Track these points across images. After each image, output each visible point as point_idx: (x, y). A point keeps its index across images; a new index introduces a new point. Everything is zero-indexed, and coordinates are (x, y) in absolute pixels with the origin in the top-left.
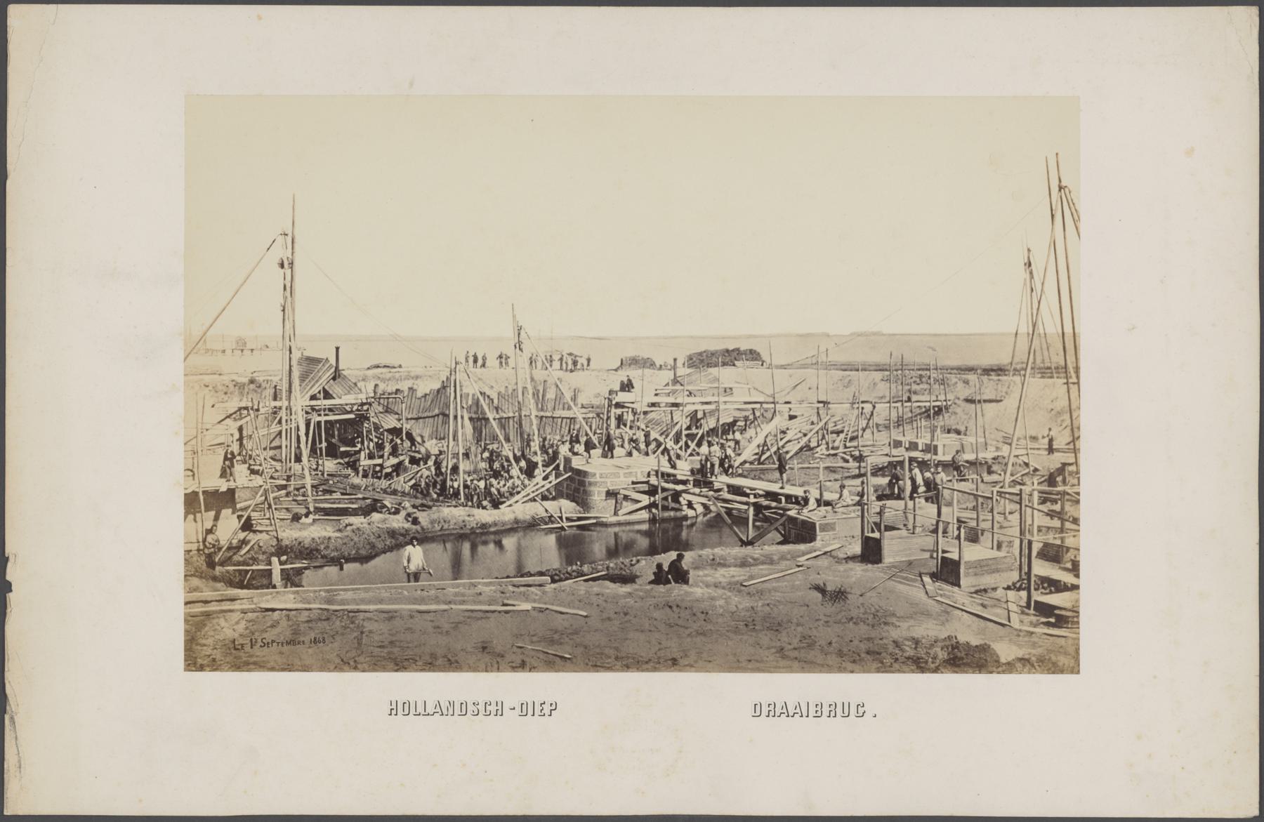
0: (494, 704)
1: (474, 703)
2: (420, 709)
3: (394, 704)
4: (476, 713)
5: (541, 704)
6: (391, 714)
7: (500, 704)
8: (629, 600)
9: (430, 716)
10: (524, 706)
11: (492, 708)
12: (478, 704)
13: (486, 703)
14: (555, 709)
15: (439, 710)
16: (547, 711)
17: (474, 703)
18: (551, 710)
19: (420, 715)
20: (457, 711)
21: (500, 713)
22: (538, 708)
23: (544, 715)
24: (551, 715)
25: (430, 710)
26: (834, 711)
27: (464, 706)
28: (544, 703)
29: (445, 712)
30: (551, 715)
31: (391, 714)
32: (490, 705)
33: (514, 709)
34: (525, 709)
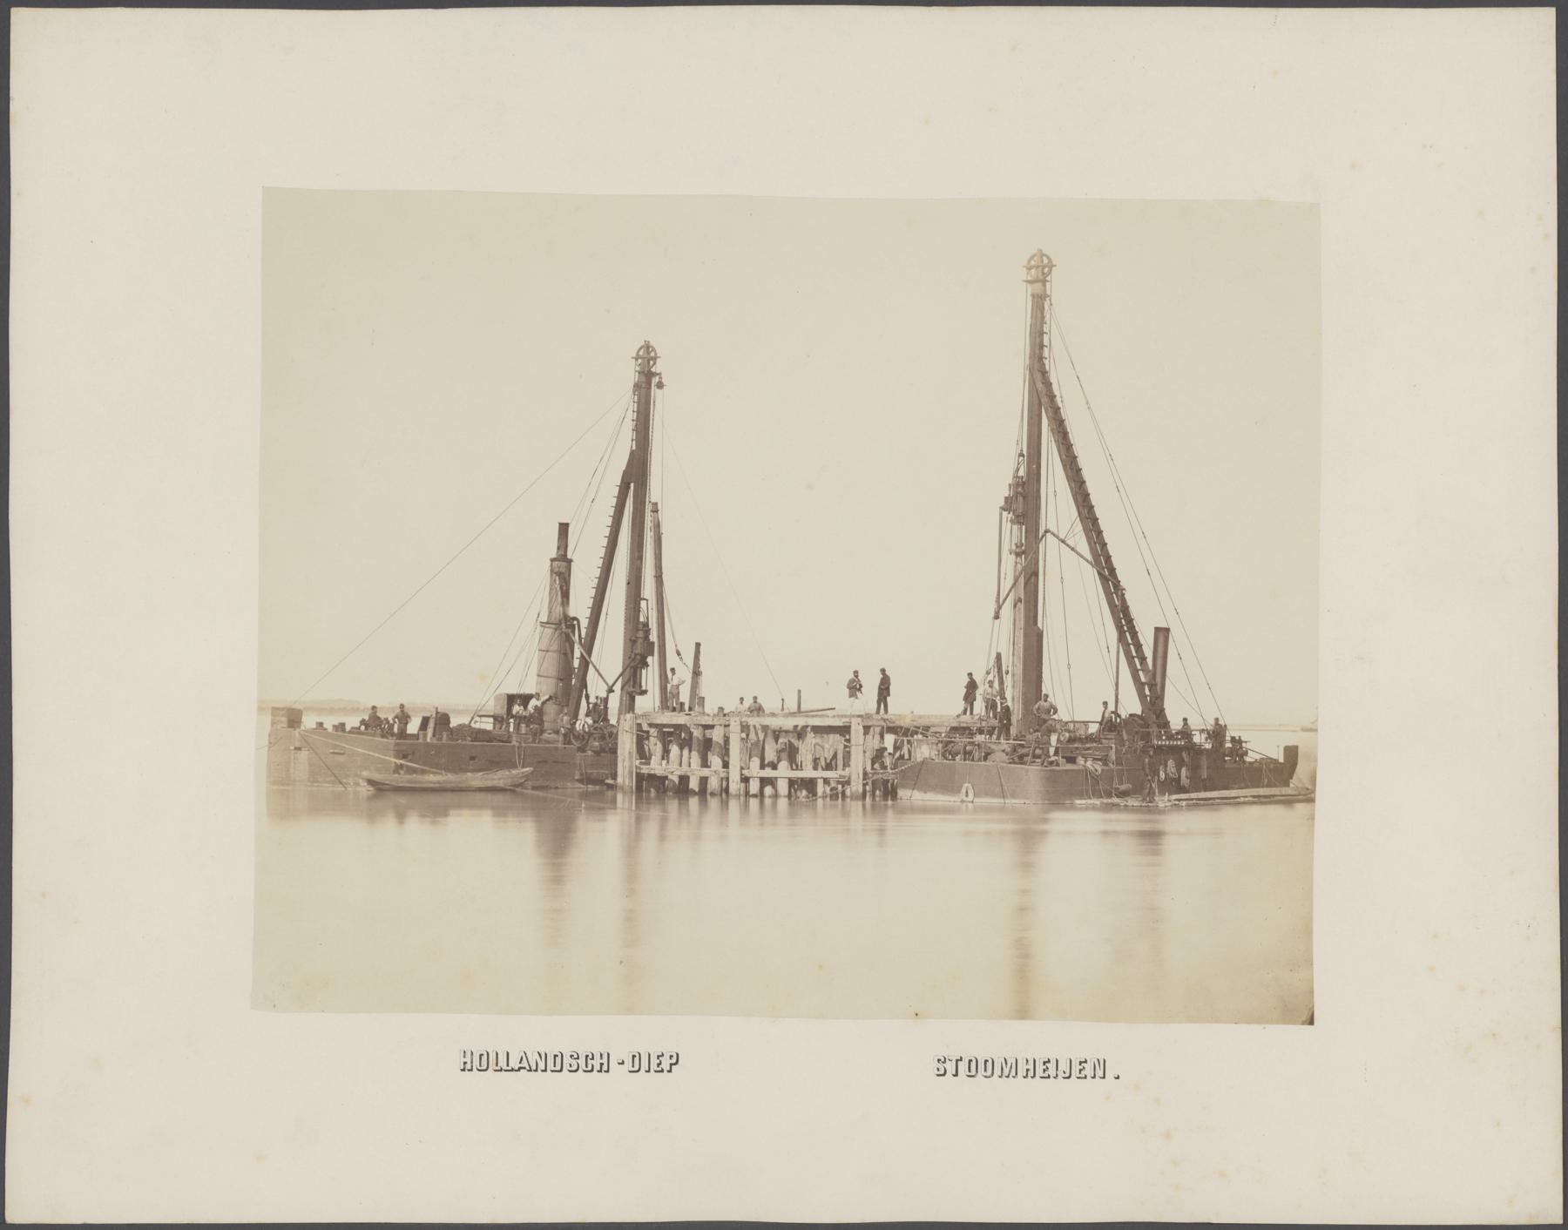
0: (597, 1056)
2: (502, 1063)
9: (514, 1073)
13: (587, 1056)
14: (677, 1063)
16: (665, 1065)
18: (671, 1065)
19: (501, 1070)
22: (654, 1061)
24: (670, 1071)
25: (514, 1063)
30: (670, 1071)
34: (637, 1063)
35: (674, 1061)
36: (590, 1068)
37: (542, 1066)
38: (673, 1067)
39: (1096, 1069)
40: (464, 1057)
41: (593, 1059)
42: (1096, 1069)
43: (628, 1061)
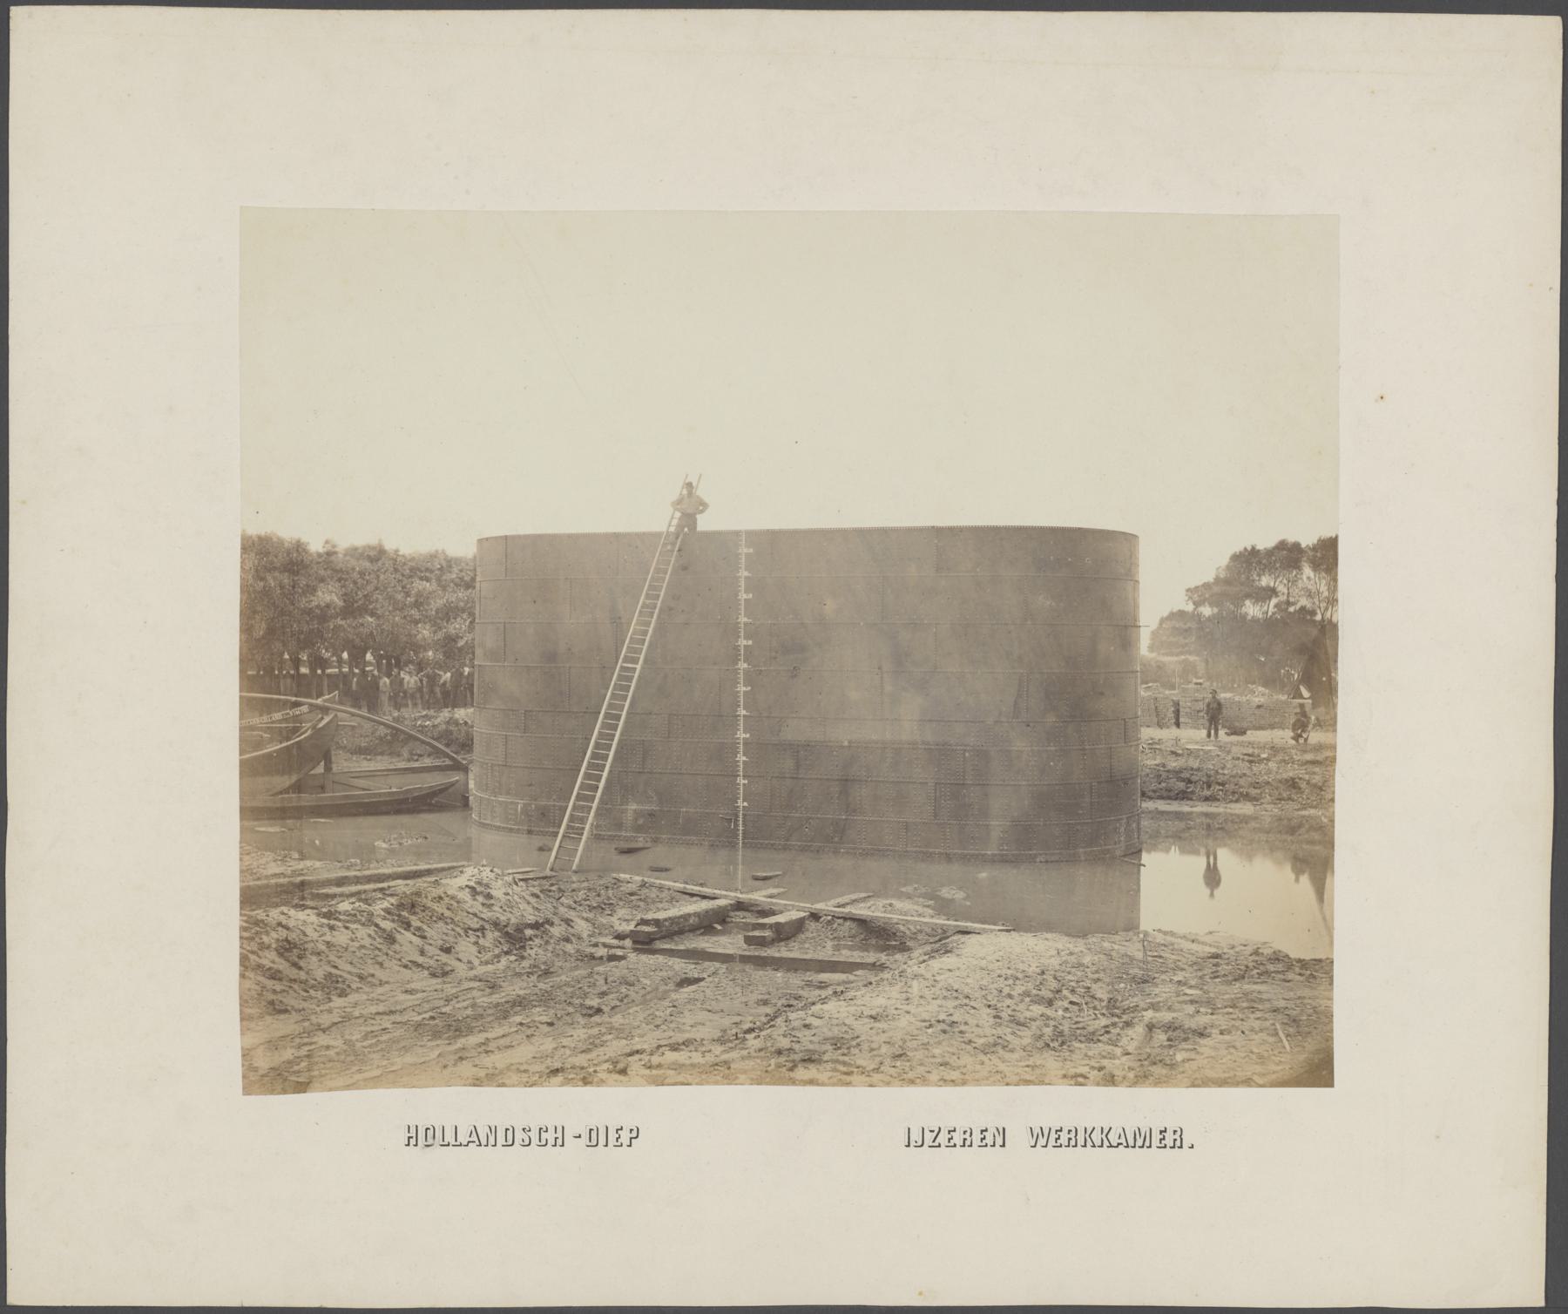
0: (552, 1130)
1: (524, 1129)
2: (449, 1138)
3: (413, 1130)
4: (527, 1143)
5: (617, 1130)
6: (408, 1145)
7: (559, 1130)
8: (318, 864)
10: (594, 1134)
11: (550, 1136)
12: (530, 1131)
13: (541, 1129)
15: (476, 1139)
16: (625, 1139)
17: (524, 1129)
18: (631, 1138)
19: (448, 1145)
20: (501, 1140)
21: (559, 1142)
22: (612, 1136)
23: (621, 1145)
24: (630, 1146)
25: (463, 1138)
26: (1074, 1139)
27: (510, 1133)
28: (622, 1129)
29: (484, 1142)
30: (630, 1146)
31: (408, 1145)
32: (547, 1131)
33: (580, 1137)
34: (593, 1138)
35: (634, 1134)
36: (543, 1142)
37: (492, 1141)
38: (633, 1140)
39: (1173, 1140)
40: (409, 1132)
41: (547, 1131)
42: (1173, 1140)
43: (585, 1136)
